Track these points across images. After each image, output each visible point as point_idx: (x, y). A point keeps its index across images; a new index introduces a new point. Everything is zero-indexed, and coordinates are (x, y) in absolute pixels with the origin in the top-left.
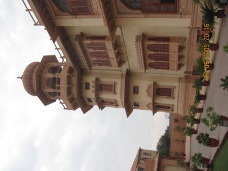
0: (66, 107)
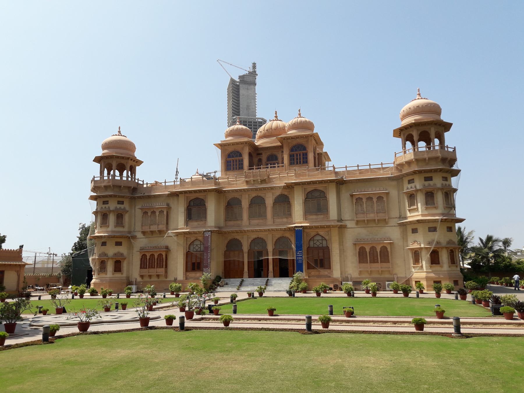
0: (96, 179)
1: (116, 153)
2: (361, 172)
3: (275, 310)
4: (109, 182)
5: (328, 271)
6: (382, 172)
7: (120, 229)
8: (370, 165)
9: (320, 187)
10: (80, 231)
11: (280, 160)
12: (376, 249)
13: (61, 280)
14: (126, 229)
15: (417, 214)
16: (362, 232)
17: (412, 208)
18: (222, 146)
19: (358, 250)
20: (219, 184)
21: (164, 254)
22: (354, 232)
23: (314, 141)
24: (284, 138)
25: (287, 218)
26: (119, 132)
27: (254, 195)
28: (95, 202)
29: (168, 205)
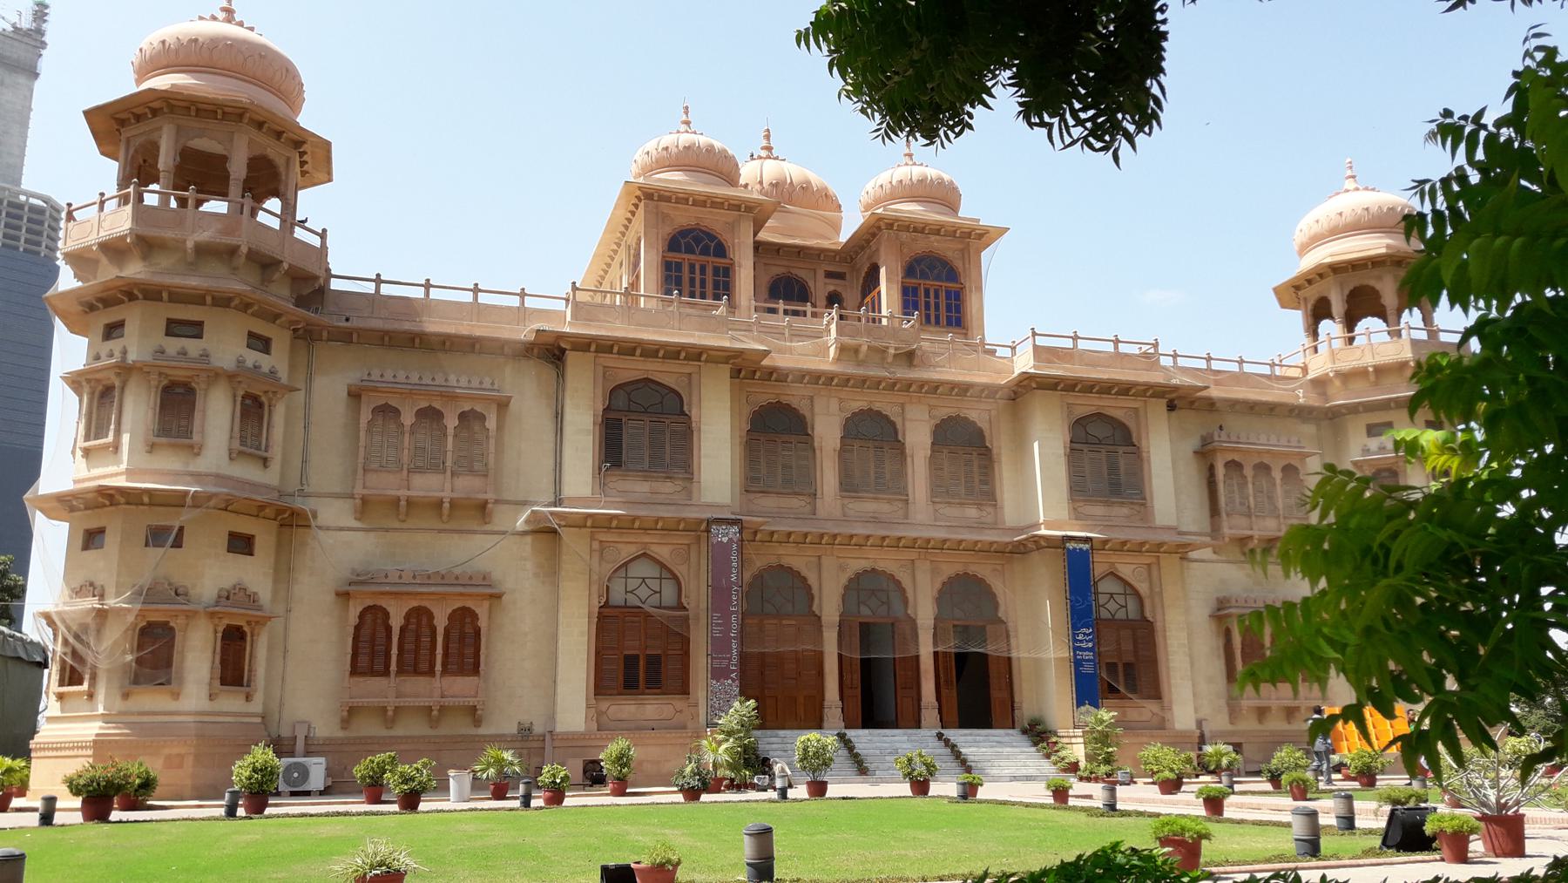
7: (248, 471)
9: (1116, 407)
14: (271, 477)
25: (979, 506)
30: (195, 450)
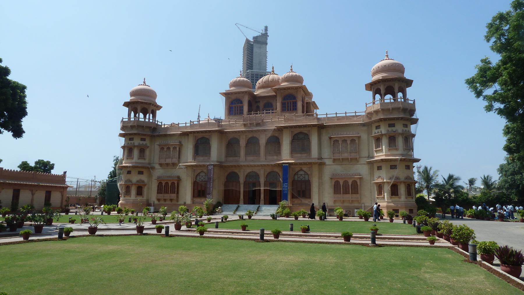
0: (124, 120)
1: (141, 99)
2: (339, 118)
3: (247, 226)
4: (134, 123)
5: (309, 200)
6: (355, 119)
8: (346, 113)
9: (305, 130)
10: (114, 162)
11: (275, 107)
12: (348, 182)
13: (98, 201)
14: (147, 161)
15: (382, 154)
16: (338, 169)
17: (378, 149)
18: (227, 95)
19: (333, 183)
20: (222, 126)
21: (176, 182)
22: (331, 169)
23: (302, 92)
24: (278, 89)
25: (277, 156)
26: (144, 82)
27: (250, 136)
28: (123, 139)
29: (180, 142)
30: (133, 158)
